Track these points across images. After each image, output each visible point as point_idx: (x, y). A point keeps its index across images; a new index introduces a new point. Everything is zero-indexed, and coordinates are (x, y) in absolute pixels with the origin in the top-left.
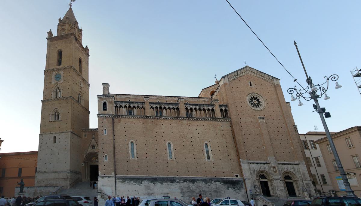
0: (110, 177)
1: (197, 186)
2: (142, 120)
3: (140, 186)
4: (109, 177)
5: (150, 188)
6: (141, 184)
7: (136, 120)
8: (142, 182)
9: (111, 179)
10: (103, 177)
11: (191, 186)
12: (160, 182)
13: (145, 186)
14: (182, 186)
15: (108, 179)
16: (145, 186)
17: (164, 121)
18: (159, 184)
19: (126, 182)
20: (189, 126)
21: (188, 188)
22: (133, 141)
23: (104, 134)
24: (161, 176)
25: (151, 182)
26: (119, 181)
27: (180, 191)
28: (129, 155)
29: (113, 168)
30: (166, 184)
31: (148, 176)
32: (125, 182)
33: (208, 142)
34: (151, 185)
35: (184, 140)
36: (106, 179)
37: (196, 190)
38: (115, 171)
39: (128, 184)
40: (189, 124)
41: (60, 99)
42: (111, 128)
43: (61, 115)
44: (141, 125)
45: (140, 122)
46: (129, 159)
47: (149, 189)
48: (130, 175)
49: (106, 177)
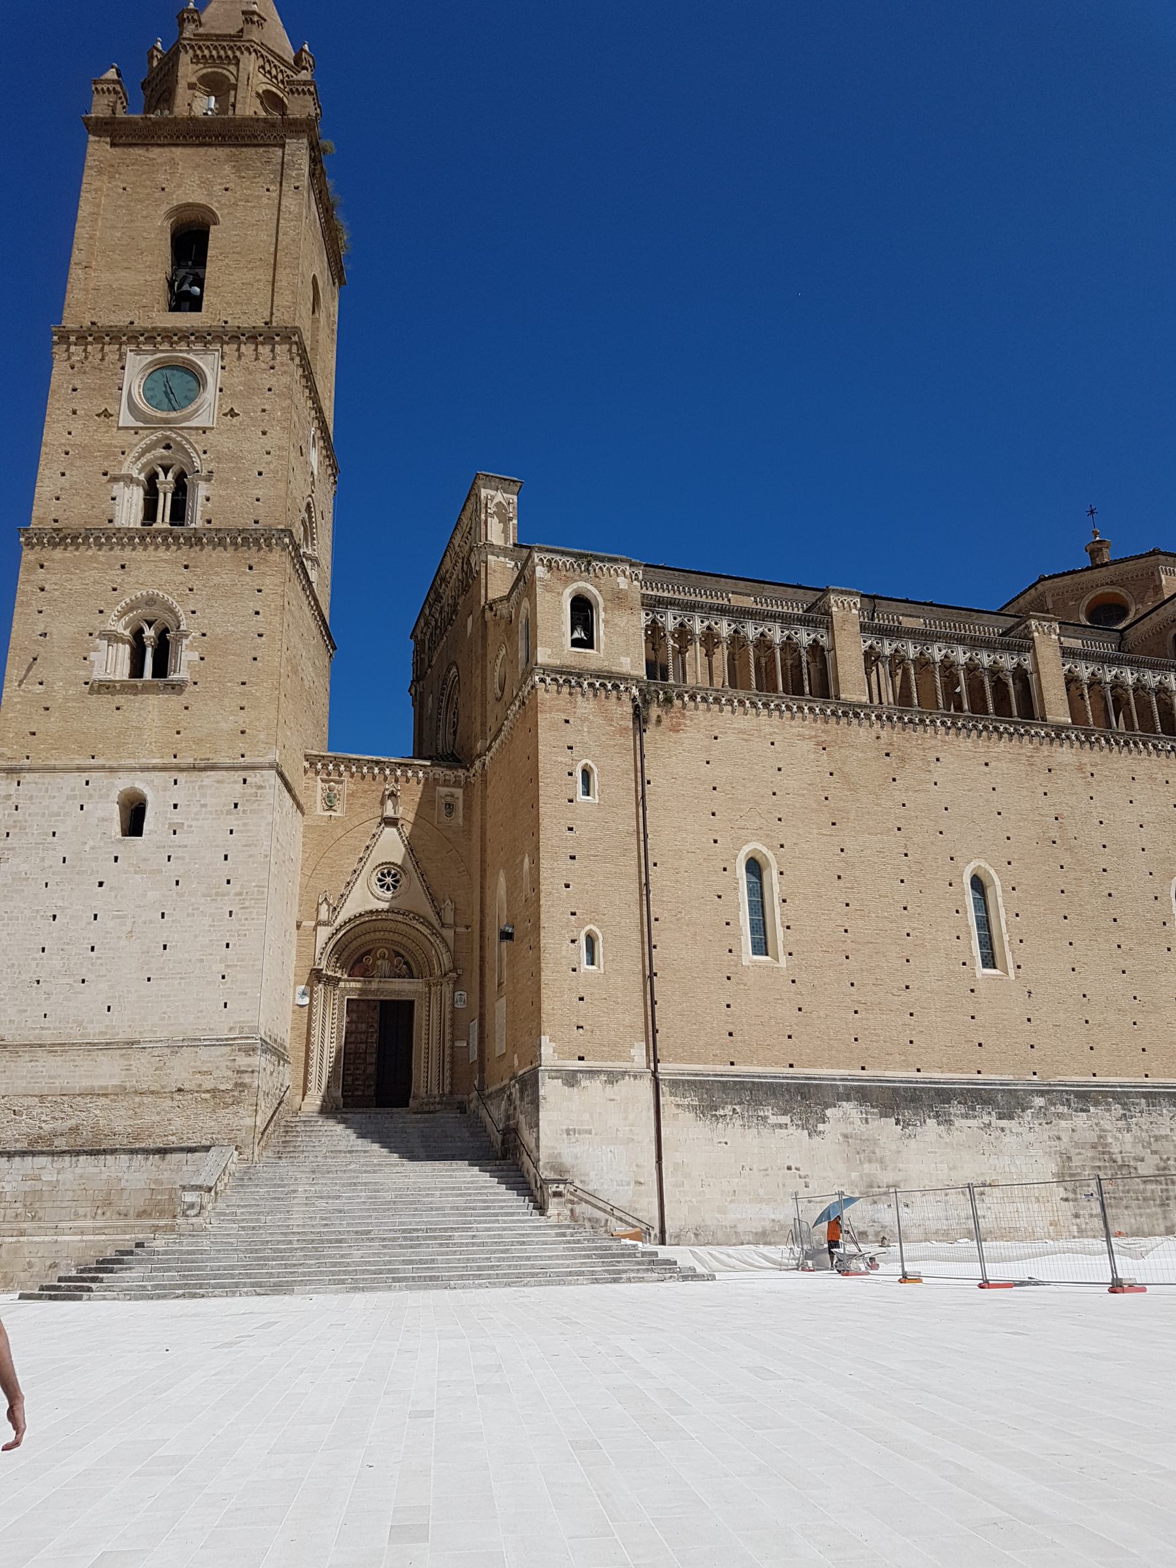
0: (624, 1073)
4: (613, 1077)
5: (879, 1155)
6: (821, 1127)
8: (829, 1112)
10: (571, 1079)
11: (1117, 1139)
12: (937, 1116)
13: (846, 1136)
14: (1065, 1139)
15: (609, 1086)
16: (846, 1136)
18: (931, 1122)
19: (728, 1111)
21: (1100, 1146)
24: (937, 1075)
25: (884, 1115)
27: (1051, 1167)
28: (738, 937)
29: (635, 1017)
30: (971, 1122)
32: (721, 1112)
34: (886, 1129)
36: (594, 1087)
37: (1142, 1160)
38: (652, 1033)
39: (739, 1122)
41: (195, 540)
43: (191, 647)
46: (737, 964)
48: (745, 1063)
49: (592, 1073)
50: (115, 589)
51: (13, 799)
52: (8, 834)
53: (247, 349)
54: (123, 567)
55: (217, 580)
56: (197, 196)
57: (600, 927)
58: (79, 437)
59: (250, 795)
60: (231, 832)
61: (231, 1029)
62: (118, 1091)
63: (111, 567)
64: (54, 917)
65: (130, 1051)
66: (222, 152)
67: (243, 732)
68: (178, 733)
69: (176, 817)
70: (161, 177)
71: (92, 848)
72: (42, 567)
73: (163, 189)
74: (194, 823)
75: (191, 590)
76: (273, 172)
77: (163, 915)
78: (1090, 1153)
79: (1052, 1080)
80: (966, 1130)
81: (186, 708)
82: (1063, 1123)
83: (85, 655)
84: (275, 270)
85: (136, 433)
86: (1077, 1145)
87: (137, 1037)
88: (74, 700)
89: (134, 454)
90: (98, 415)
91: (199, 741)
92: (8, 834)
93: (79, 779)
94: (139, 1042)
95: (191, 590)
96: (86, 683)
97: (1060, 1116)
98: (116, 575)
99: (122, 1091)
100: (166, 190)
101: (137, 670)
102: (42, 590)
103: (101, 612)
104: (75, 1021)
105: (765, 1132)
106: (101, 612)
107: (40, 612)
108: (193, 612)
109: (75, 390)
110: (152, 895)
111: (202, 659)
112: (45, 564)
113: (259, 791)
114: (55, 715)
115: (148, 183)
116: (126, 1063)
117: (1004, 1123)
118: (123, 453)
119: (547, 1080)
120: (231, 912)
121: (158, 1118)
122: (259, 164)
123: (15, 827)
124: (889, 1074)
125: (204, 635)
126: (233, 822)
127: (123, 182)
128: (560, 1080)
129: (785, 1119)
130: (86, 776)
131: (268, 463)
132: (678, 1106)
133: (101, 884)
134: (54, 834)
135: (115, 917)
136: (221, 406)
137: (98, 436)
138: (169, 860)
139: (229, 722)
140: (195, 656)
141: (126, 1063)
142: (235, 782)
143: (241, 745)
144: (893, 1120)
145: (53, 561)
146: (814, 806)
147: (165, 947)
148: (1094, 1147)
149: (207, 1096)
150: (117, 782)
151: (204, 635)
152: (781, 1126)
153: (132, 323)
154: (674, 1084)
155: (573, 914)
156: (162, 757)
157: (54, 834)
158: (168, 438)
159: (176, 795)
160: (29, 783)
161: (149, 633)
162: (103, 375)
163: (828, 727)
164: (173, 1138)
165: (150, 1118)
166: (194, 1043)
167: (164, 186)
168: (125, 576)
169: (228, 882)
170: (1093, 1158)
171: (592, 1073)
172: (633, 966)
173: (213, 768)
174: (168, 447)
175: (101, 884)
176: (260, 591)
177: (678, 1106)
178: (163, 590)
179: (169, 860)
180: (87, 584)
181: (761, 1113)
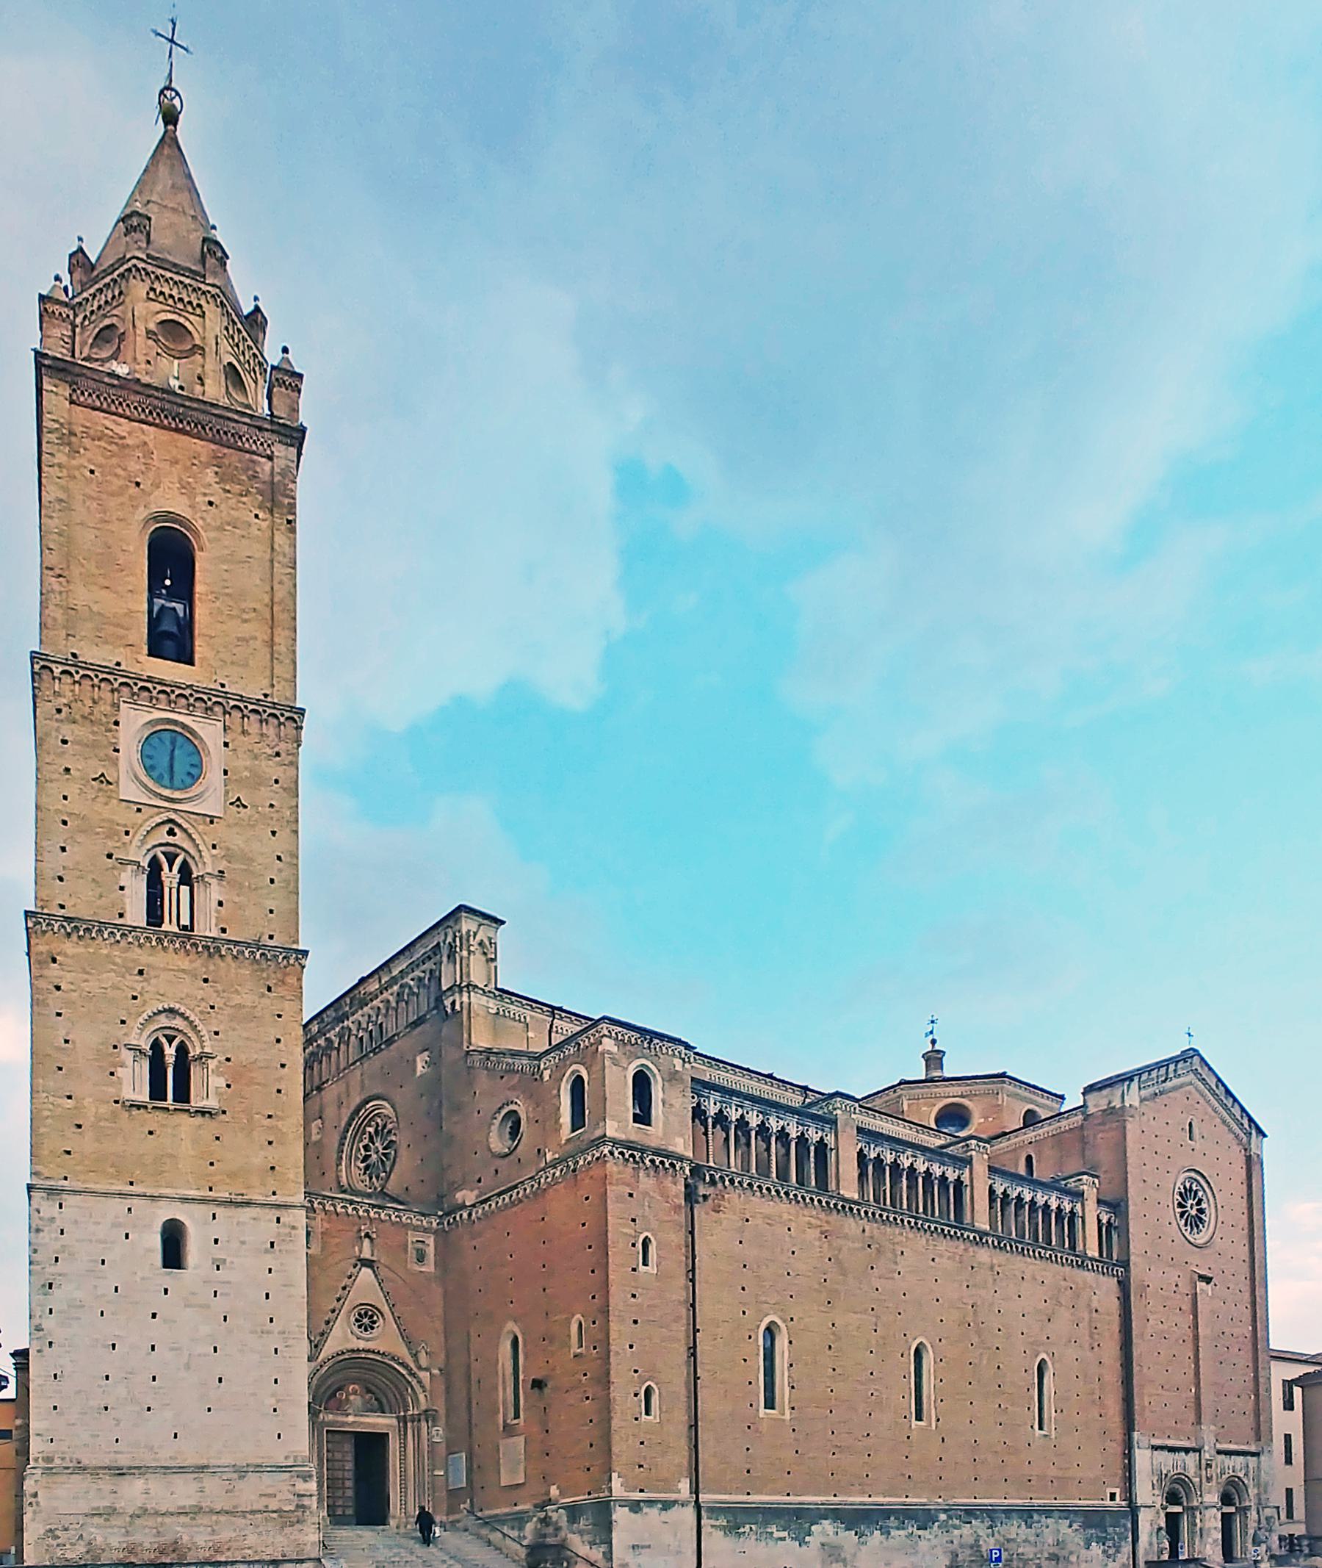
0: (675, 1502)
1: (1002, 1539)
2: (822, 1215)
3: (804, 1547)
4: (667, 1505)
5: (843, 1556)
6: (807, 1539)
7: (793, 1208)
8: (813, 1528)
9: (675, 1512)
10: (635, 1506)
17: (911, 1235)
18: (877, 1533)
20: (996, 1277)
22: (779, 1322)
23: (642, 1268)
24: (881, 1500)
25: (848, 1529)
26: (713, 1522)
29: (681, 1457)
30: (902, 1532)
31: (832, 1498)
32: (742, 1530)
33: (1048, 1355)
35: (975, 1340)
36: (653, 1513)
40: (997, 1269)
42: (678, 1238)
44: (817, 1243)
45: (810, 1225)
47: (837, 1561)
49: (651, 1503)
50: (135, 998)
51: (58, 1222)
52: (57, 1259)
53: (253, 724)
54: (141, 972)
55: (236, 999)
56: (179, 506)
57: (657, 1384)
58: (74, 805)
59: (286, 1235)
60: (270, 1271)
61: (286, 1458)
62: (196, 1510)
63: (129, 970)
64: (114, 1346)
65: (202, 1475)
66: (202, 448)
67: (273, 1168)
68: (212, 1164)
69: (218, 1252)
70: (134, 466)
71: (143, 1279)
72: (54, 960)
73: (138, 484)
74: (235, 1260)
75: (212, 1007)
76: (260, 492)
77: (215, 1349)
78: (968, 1552)
79: (951, 1502)
80: (898, 1538)
81: (218, 1138)
82: (956, 1532)
83: (112, 1070)
84: (272, 628)
85: (139, 810)
86: (961, 1546)
87: (204, 1462)
88: (106, 1120)
89: (139, 837)
90: (94, 780)
91: (232, 1175)
92: (57, 1259)
93: (119, 1206)
94: (207, 1467)
95: (212, 1007)
96: (116, 1102)
97: (955, 1527)
98: (137, 984)
99: (197, 1511)
100: (142, 486)
101: (157, 1091)
102: (58, 988)
103: (123, 1022)
104: (146, 1446)
105: (771, 1543)
106: (123, 1022)
107: (59, 1014)
108: (216, 1033)
109: (65, 742)
110: (205, 1329)
111: (228, 1086)
112: (58, 958)
113: (293, 1232)
114: (88, 1134)
115: (119, 471)
116: (200, 1485)
117: (920, 1532)
118: (127, 833)
119: (618, 1508)
120: (276, 1350)
121: (234, 1535)
122: (244, 478)
123: (64, 1252)
124: (851, 1499)
125: (228, 1060)
126: (269, 1260)
127: (90, 461)
128: (627, 1509)
129: (785, 1534)
130: (128, 1203)
131: (280, 871)
132: (712, 1526)
133: (154, 1316)
134: (103, 1262)
135: (172, 1349)
136: (227, 793)
137: (98, 807)
138: (215, 1296)
139: (259, 1158)
140: (222, 1082)
141: (200, 1485)
142: (270, 1221)
143: (272, 1184)
144: (853, 1532)
145: (66, 955)
146: (817, 1286)
147: (220, 1380)
148: (972, 1547)
149: (275, 1515)
150: (160, 1212)
151: (228, 1060)
152: (783, 1539)
153: (118, 664)
154: (711, 1510)
155: (636, 1371)
157: (103, 1262)
158: (171, 821)
159: (217, 1230)
160: (70, 1206)
161: (170, 1051)
162: (95, 729)
163: (830, 1218)
164: (249, 1552)
165: (225, 1535)
166: (259, 1469)
167: (138, 480)
168: (145, 984)
169: (271, 1320)
170: (971, 1555)
171: (651, 1503)
172: (682, 1417)
173: (248, 1204)
174: (171, 832)
175: (154, 1316)
176: (279, 1016)
177: (712, 1526)
178: (185, 1005)
179: (215, 1296)
180: (106, 989)
181: (769, 1530)
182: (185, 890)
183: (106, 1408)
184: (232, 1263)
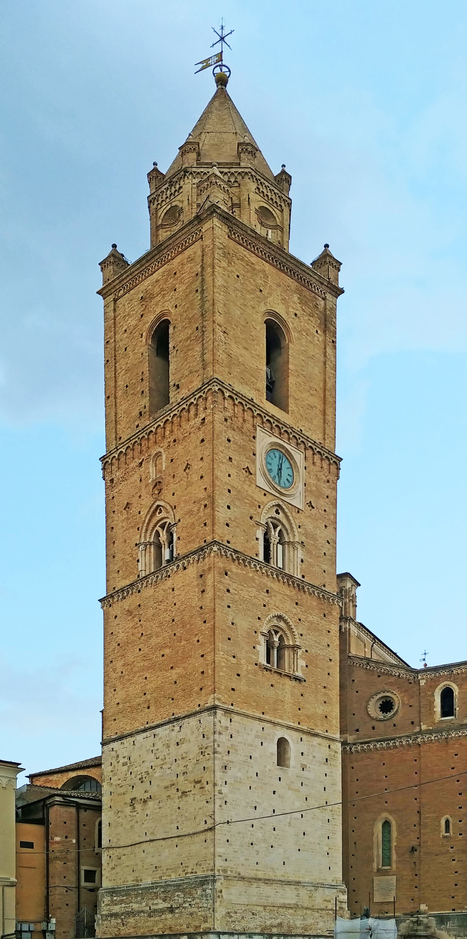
51: (229, 731)
59: (332, 756)
72: (226, 574)
74: (311, 766)
93: (257, 726)
111: (307, 666)
112: (229, 573)
133: (274, 792)
139: (321, 710)
143: (326, 726)
145: (231, 572)
150: (277, 732)
156: (294, 723)
180: (251, 597)
182: (280, 547)
183: (252, 844)
184: (309, 768)
